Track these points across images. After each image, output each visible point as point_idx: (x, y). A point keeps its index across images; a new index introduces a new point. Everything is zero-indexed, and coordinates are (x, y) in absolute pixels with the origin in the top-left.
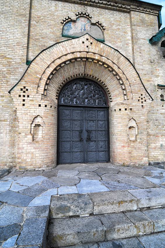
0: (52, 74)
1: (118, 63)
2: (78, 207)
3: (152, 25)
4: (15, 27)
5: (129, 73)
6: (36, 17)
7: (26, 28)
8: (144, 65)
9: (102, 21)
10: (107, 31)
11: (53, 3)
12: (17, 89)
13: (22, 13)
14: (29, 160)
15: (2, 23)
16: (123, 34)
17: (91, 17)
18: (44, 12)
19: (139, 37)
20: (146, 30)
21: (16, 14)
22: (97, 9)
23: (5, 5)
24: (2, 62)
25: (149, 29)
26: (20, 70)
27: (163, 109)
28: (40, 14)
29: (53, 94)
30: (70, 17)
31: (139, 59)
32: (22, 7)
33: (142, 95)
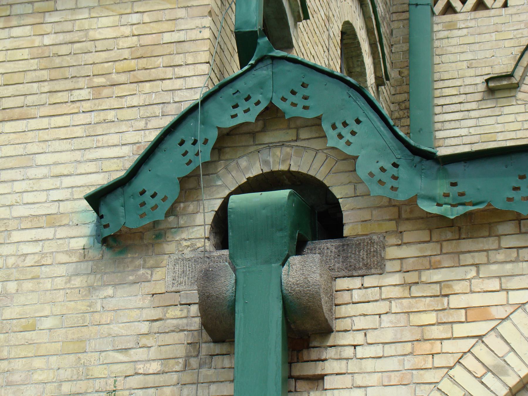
3: (141, 75)
20: (79, 132)
25: (111, 115)
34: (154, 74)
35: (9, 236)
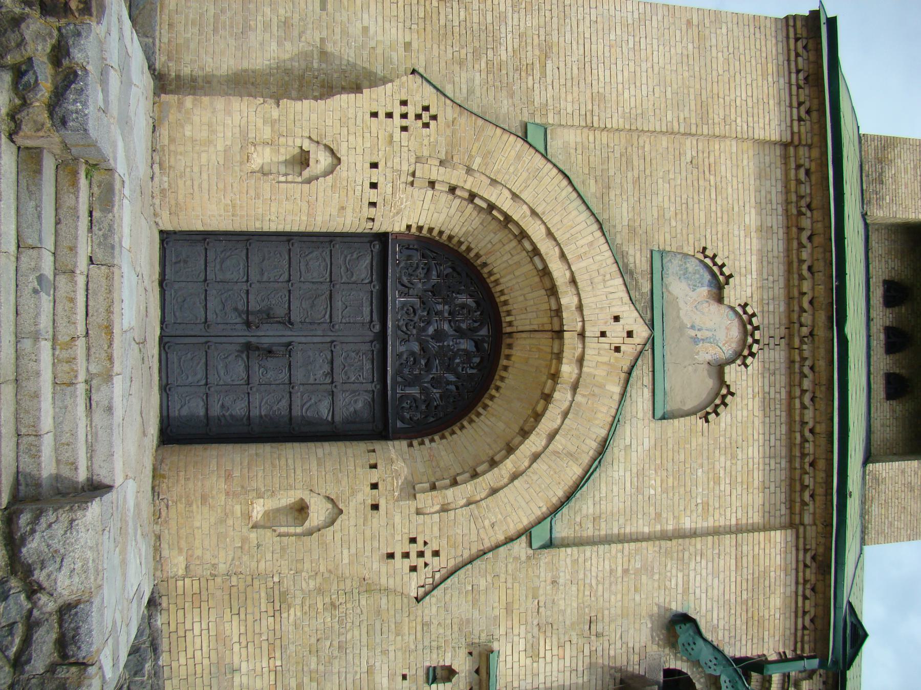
0: (492, 207)
1: (556, 453)
2: (109, 231)
3: (750, 624)
4: (657, 89)
5: (519, 498)
6: (712, 160)
7: (658, 124)
8: (574, 588)
9: (739, 407)
10: (699, 429)
11: (775, 220)
12: (428, 95)
13: (710, 111)
14: (188, 134)
15: (667, 49)
16: (699, 501)
17: (746, 366)
18: (735, 187)
20: (727, 597)
21: (704, 92)
22: (783, 390)
23: (731, 56)
24: (529, 48)
25: (733, 612)
26: (505, 102)
27: (391, 677)
28: (723, 174)
29: (424, 213)
30: (731, 280)
31: (600, 568)
32: (733, 110)
34: (750, 629)
35: (681, 571)
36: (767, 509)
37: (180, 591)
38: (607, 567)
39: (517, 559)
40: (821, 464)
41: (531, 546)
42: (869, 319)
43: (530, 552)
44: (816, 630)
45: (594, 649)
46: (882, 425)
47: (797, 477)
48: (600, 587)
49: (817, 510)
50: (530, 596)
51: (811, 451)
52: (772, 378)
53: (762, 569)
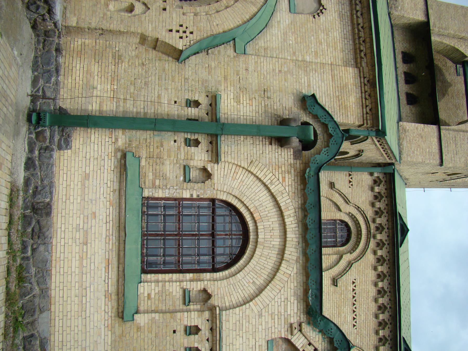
3: (341, 107)
8: (256, 74)
16: (313, 50)
19: (311, 74)
20: (329, 92)
25: (332, 100)
27: (169, 101)
31: (268, 67)
33: (192, 33)
34: (341, 110)
36: (345, 60)
37: (72, 49)
38: (271, 67)
39: (228, 56)
40: (368, 40)
41: (235, 52)
42: (396, 68)
43: (235, 54)
44: (372, 114)
45: (266, 104)
46: (406, 116)
47: (358, 47)
48: (268, 76)
49: (368, 61)
50: (236, 74)
51: (363, 36)
52: (343, 6)
53: (344, 83)
